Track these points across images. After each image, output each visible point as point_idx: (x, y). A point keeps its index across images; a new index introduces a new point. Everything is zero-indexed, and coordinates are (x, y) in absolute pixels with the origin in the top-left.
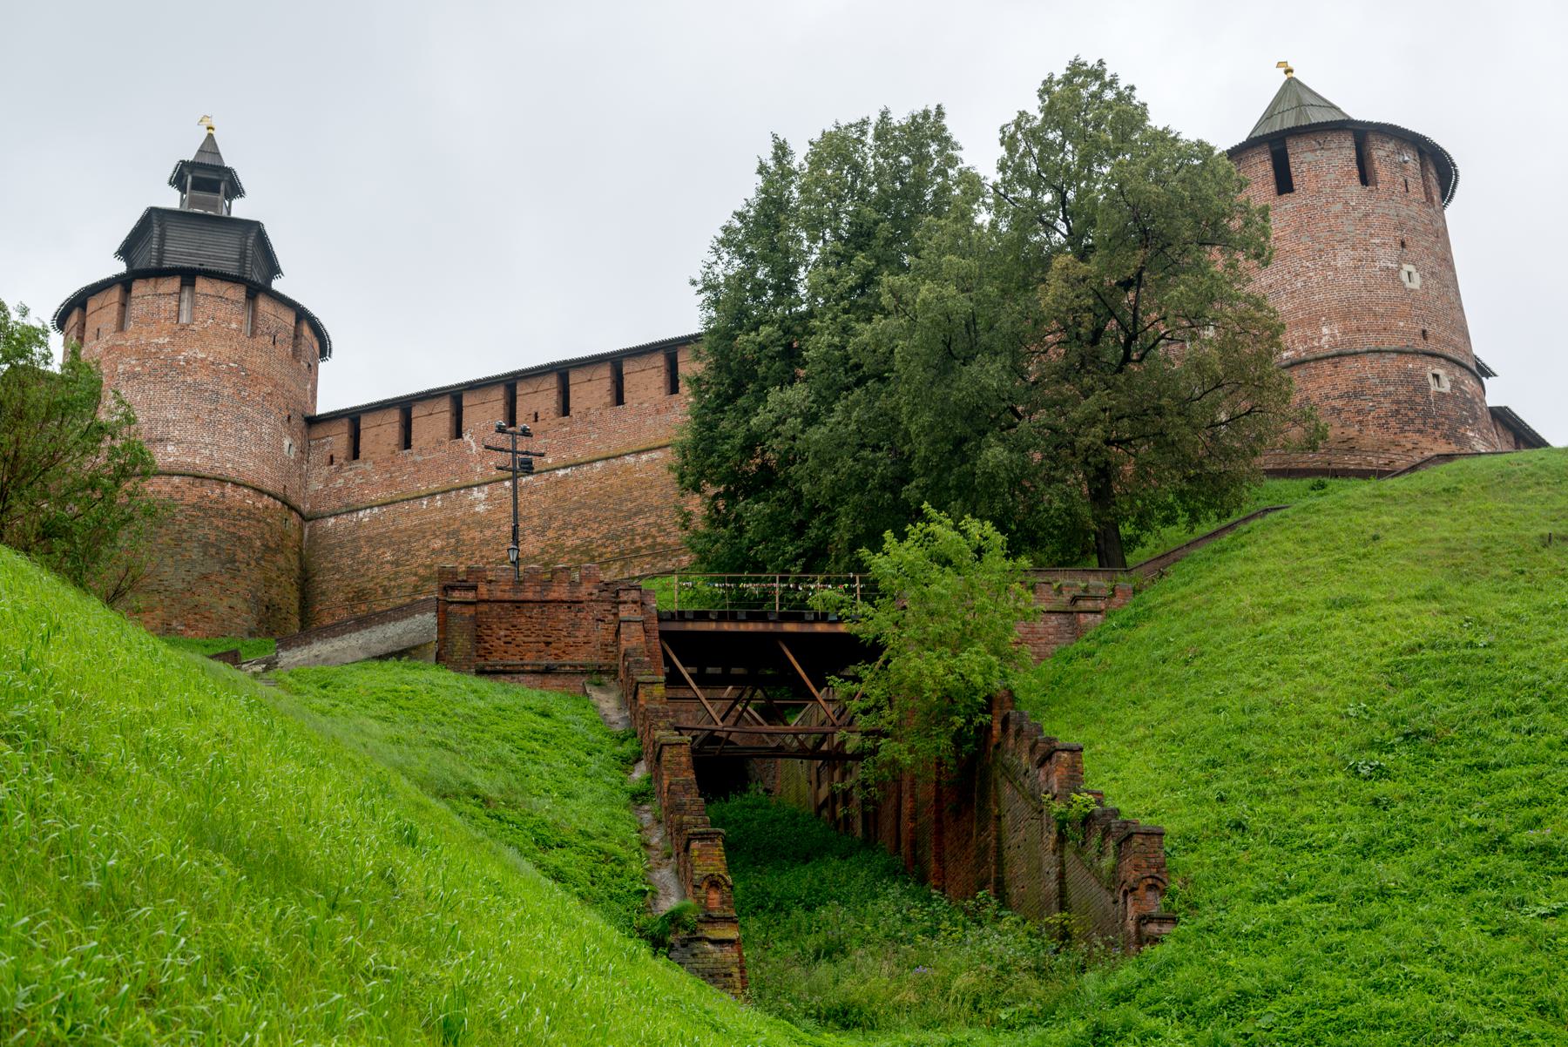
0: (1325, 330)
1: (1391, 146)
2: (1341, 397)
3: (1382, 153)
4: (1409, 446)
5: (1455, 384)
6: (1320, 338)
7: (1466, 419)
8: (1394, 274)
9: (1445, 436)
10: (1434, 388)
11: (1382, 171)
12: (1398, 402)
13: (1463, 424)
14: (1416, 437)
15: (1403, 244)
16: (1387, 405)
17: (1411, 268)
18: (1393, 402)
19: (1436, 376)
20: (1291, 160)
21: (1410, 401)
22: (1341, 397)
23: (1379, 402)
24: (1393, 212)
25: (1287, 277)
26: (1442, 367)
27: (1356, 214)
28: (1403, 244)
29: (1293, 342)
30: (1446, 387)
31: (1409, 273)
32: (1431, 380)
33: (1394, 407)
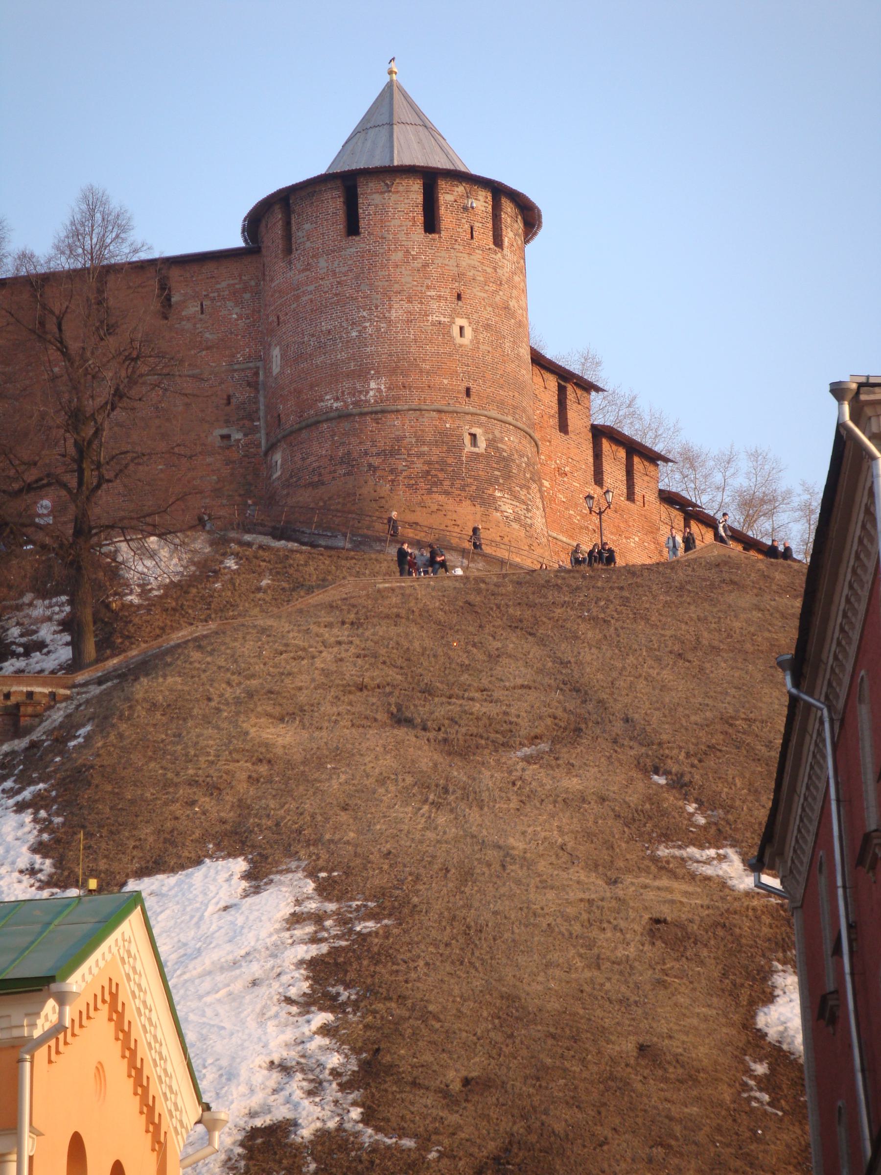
0: (373, 385)
1: (460, 189)
2: (378, 454)
3: (449, 198)
4: (435, 507)
5: (492, 443)
6: (367, 393)
7: (497, 478)
8: (443, 329)
9: (472, 499)
10: (468, 448)
11: (446, 216)
12: (430, 463)
13: (491, 484)
14: (442, 498)
15: (459, 297)
16: (419, 466)
17: (461, 321)
18: (424, 463)
19: (474, 436)
20: (360, 201)
21: (443, 463)
22: (378, 454)
23: (413, 462)
24: (452, 262)
25: (344, 324)
26: (480, 425)
27: (417, 264)
28: (459, 297)
29: (343, 392)
30: (482, 444)
31: (461, 328)
32: (467, 439)
33: (426, 468)
